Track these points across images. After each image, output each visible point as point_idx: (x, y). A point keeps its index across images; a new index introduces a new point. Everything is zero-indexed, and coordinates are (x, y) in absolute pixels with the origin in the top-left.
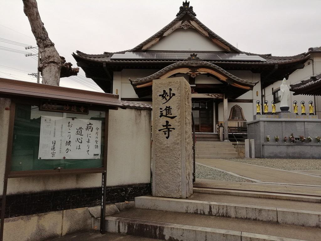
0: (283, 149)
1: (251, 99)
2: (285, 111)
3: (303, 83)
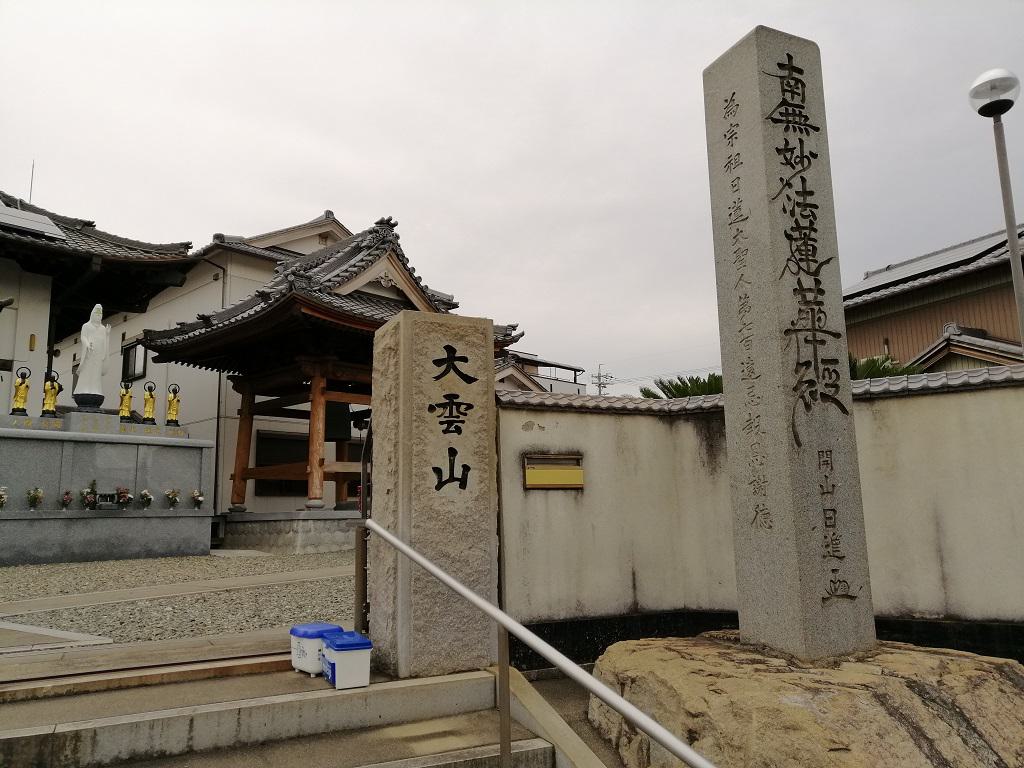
0: (53, 533)
1: (8, 358)
2: (88, 409)
3: (184, 328)
